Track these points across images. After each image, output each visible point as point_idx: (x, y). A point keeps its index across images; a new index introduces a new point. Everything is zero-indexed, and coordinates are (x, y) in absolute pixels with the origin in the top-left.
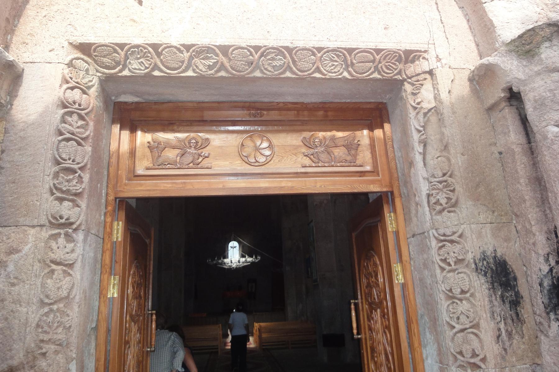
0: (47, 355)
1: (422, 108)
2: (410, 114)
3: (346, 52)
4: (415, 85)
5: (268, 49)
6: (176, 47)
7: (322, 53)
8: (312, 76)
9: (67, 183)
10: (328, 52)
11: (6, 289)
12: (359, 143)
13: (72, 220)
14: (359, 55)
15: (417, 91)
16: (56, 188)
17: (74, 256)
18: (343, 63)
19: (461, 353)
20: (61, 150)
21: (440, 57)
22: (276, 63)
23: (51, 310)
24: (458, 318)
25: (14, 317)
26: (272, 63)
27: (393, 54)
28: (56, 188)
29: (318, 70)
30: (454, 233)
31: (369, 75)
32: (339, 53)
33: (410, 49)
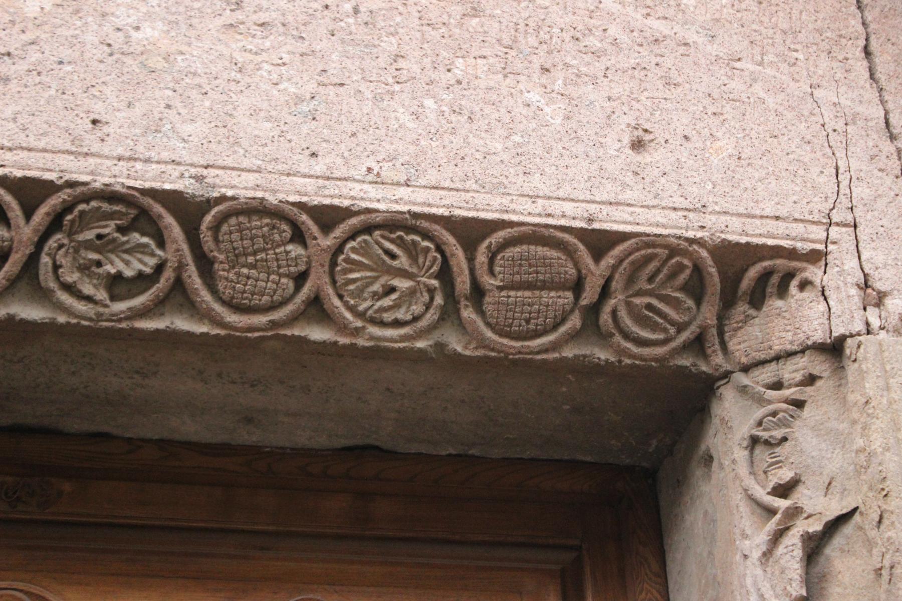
2: (745, 536)
3: (449, 239)
4: (770, 402)
5: (86, 198)
7: (339, 232)
8: (289, 332)
10: (368, 229)
14: (510, 252)
15: (778, 434)
18: (435, 283)
21: (880, 286)
22: (121, 266)
26: (99, 264)
27: (670, 257)
31: (554, 346)
32: (417, 238)
33: (743, 240)
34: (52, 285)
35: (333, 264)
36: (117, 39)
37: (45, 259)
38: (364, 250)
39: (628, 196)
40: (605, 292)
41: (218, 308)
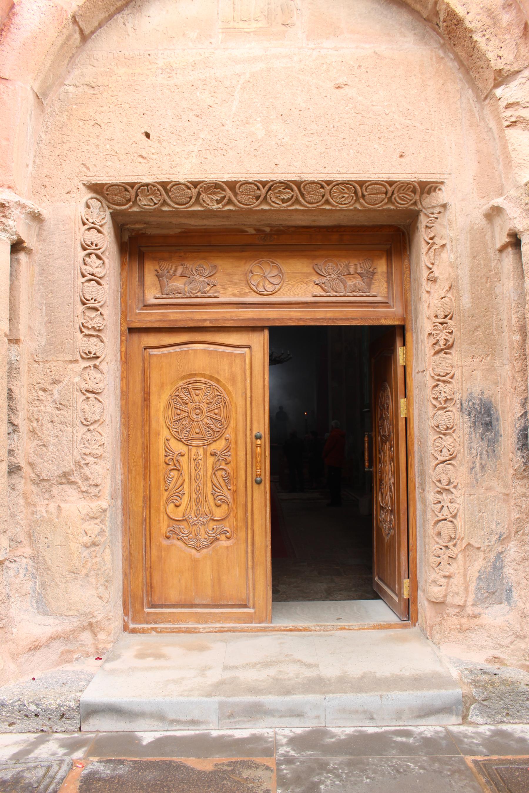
0: (89, 465)
1: (434, 243)
2: (423, 249)
3: (356, 185)
4: (430, 218)
6: (183, 184)
7: (331, 186)
9: (91, 322)
10: (338, 184)
11: (54, 412)
12: (375, 271)
13: (98, 355)
14: (370, 187)
15: (431, 225)
16: (84, 326)
17: (101, 385)
18: (353, 195)
19: (439, 481)
20: (85, 292)
22: (284, 197)
23: (89, 430)
24: (441, 451)
25: (63, 435)
28: (84, 326)
29: (327, 202)
30: (447, 374)
31: (381, 206)
33: (425, 180)
34: (270, 202)
35: (330, 192)
36: (279, 142)
37: (268, 197)
38: (337, 189)
39: (398, 171)
40: (393, 194)
41: (305, 203)
